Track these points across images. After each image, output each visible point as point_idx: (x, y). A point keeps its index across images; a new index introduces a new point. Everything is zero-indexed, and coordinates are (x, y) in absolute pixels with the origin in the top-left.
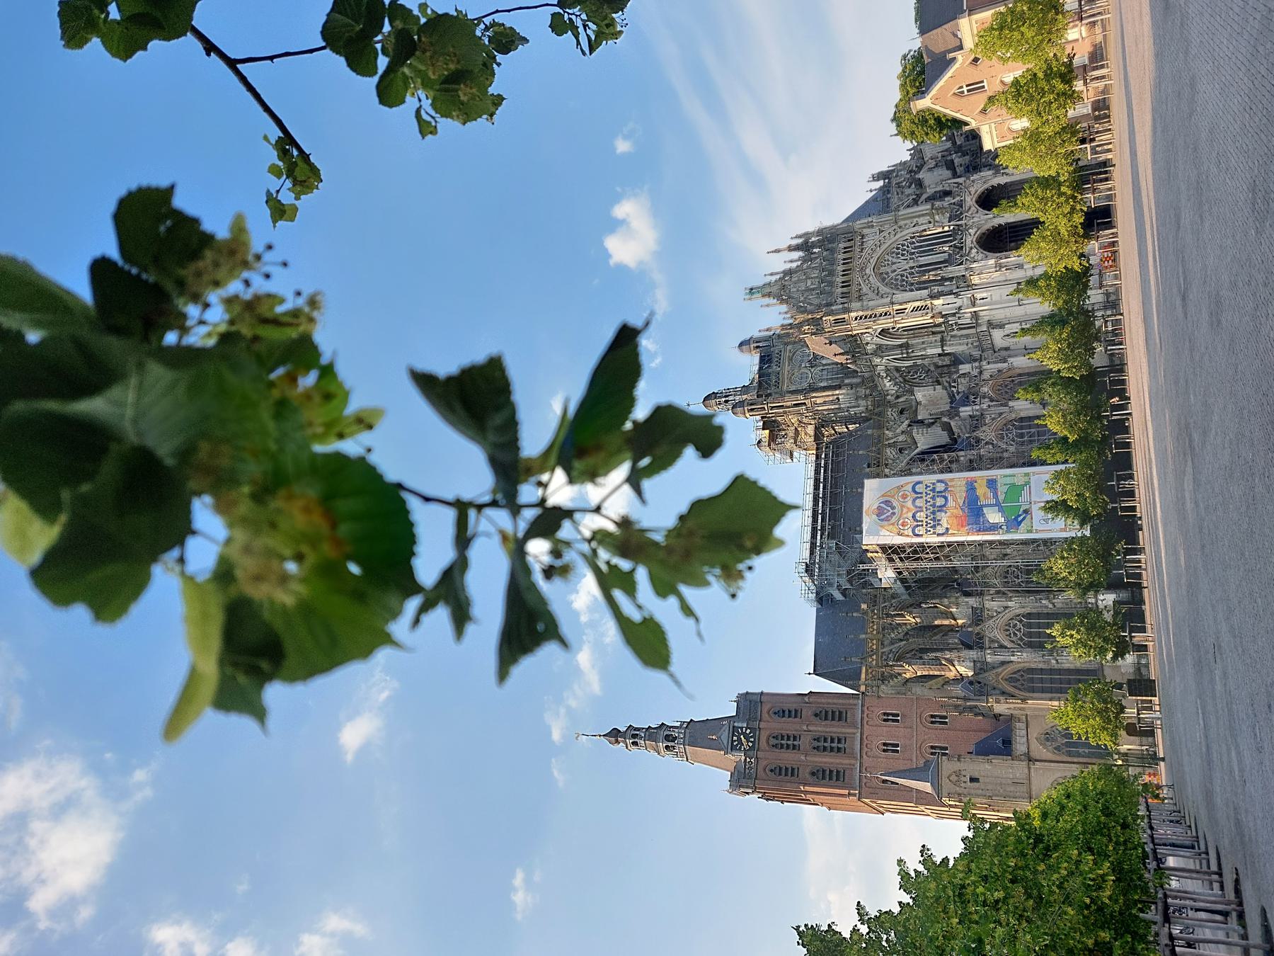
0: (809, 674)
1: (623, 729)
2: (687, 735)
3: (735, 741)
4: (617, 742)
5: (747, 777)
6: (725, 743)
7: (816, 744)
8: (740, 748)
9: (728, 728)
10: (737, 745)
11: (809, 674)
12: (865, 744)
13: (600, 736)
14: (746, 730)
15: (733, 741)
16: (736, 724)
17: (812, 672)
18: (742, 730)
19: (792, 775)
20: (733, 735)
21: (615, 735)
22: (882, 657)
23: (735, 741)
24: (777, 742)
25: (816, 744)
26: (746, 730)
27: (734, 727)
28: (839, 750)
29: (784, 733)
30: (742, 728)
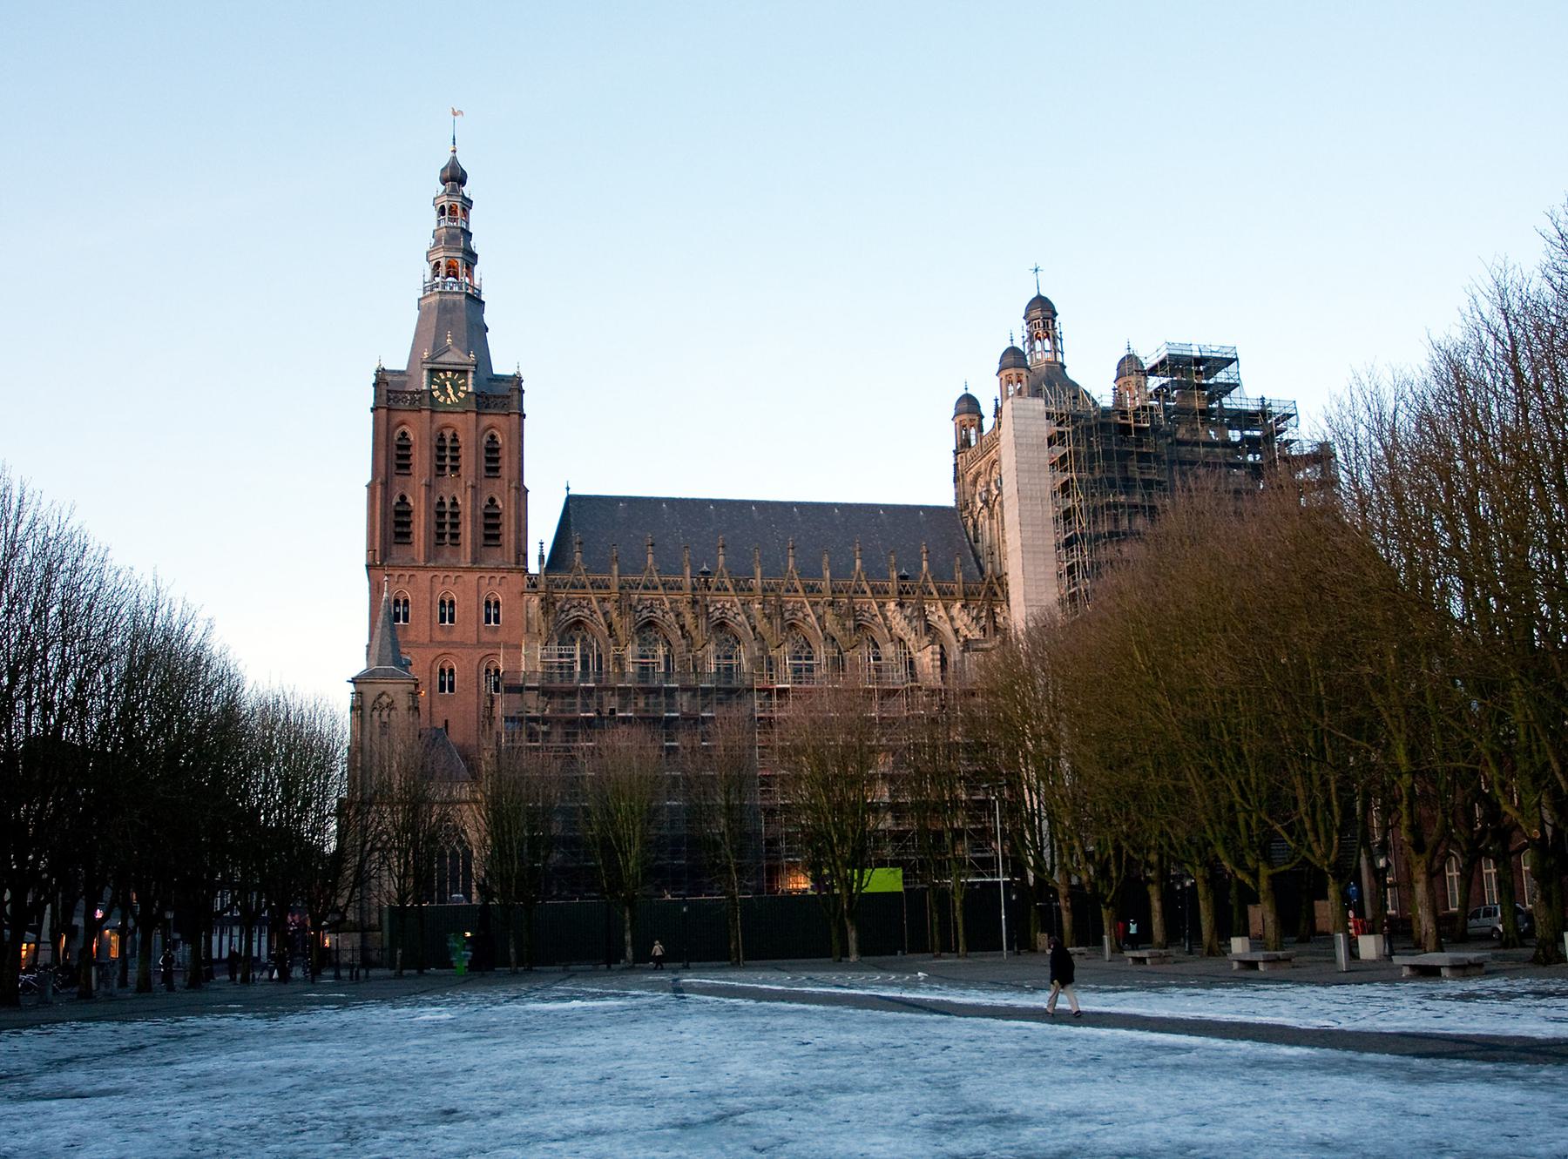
0: (568, 489)
1: (466, 190)
2: (457, 297)
3: (446, 375)
4: (444, 181)
5: (392, 396)
6: (439, 359)
7: (447, 501)
8: (436, 384)
9: (461, 361)
10: (439, 378)
11: (568, 489)
12: (450, 574)
13: (454, 151)
14: (463, 391)
15: (444, 371)
16: (470, 375)
17: (571, 492)
18: (463, 385)
19: (400, 466)
20: (454, 371)
21: (455, 177)
22: (584, 599)
23: (446, 375)
24: (448, 442)
25: (447, 501)
26: (463, 391)
27: (466, 372)
28: (441, 536)
29: (462, 451)
30: (465, 384)
